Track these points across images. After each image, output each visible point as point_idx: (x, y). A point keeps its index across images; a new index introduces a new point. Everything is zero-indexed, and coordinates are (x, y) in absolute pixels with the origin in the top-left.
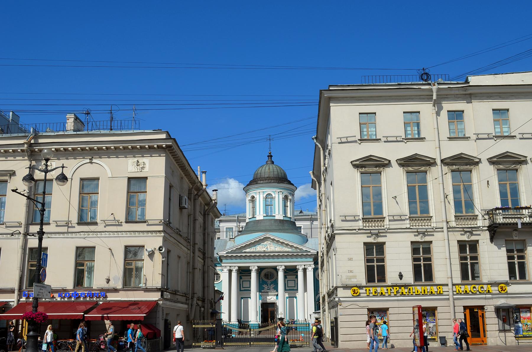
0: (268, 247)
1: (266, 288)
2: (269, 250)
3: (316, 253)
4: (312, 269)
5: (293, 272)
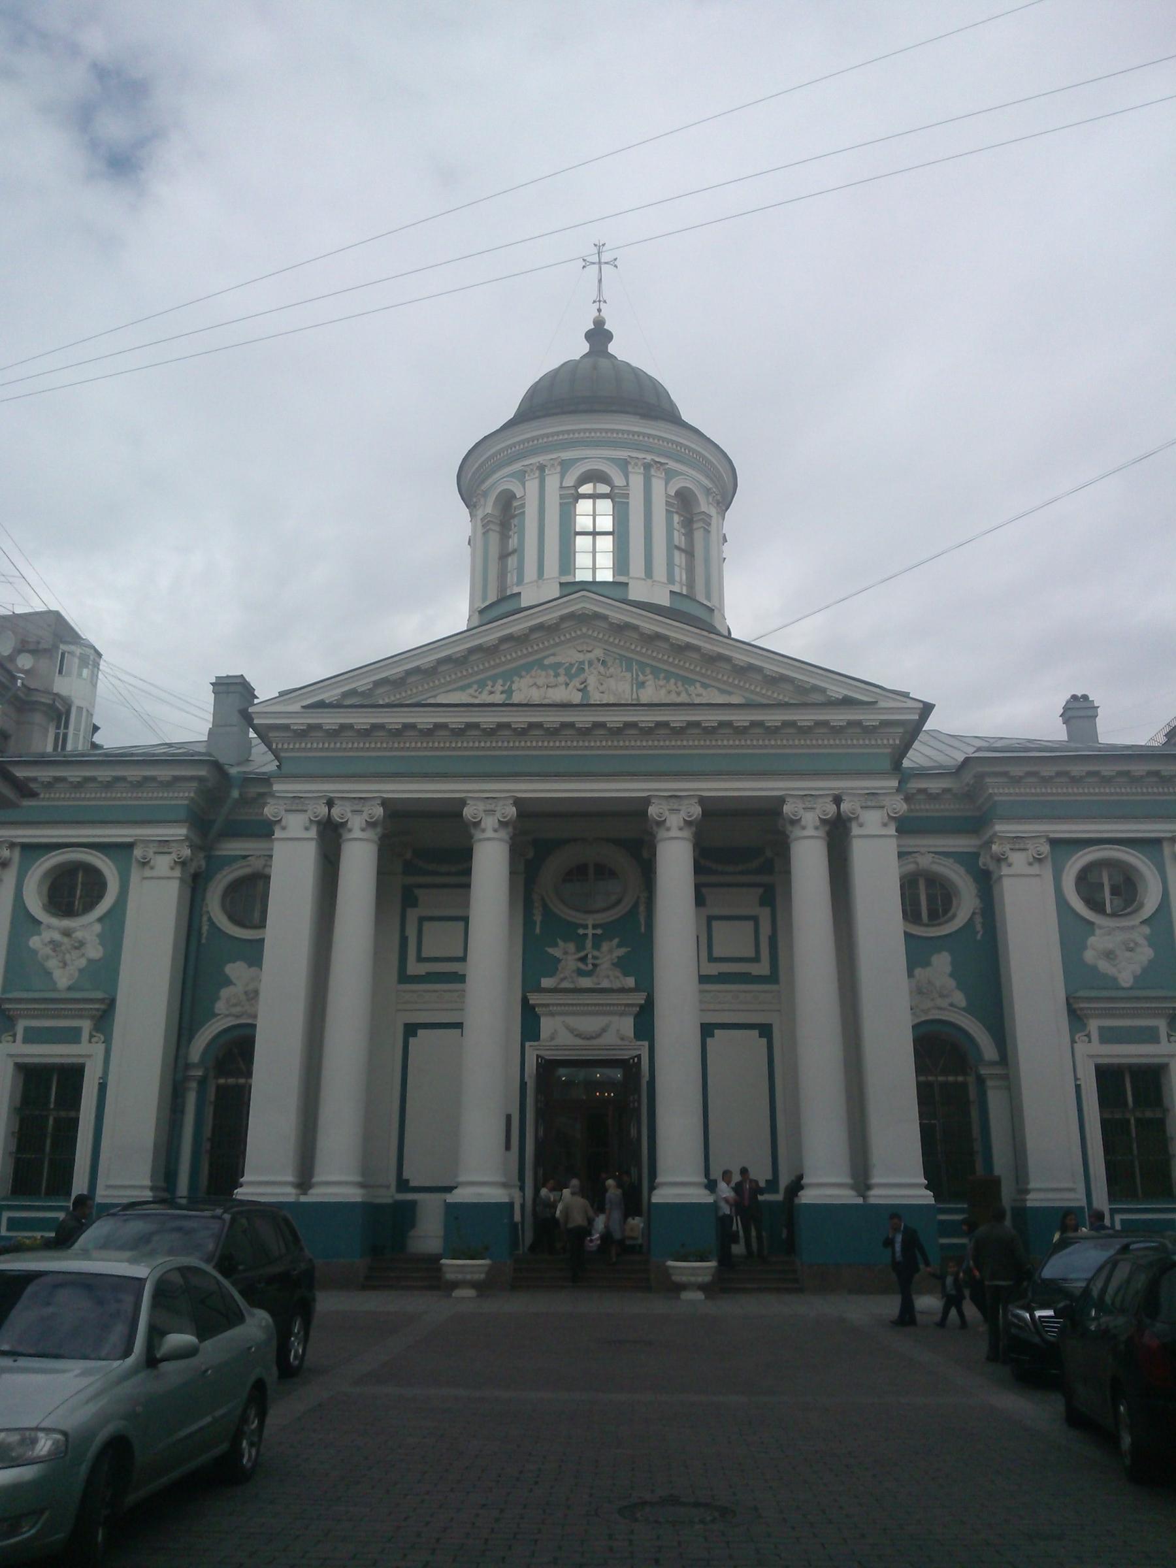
0: (592, 681)
1: (570, 963)
2: (596, 698)
4: (885, 825)
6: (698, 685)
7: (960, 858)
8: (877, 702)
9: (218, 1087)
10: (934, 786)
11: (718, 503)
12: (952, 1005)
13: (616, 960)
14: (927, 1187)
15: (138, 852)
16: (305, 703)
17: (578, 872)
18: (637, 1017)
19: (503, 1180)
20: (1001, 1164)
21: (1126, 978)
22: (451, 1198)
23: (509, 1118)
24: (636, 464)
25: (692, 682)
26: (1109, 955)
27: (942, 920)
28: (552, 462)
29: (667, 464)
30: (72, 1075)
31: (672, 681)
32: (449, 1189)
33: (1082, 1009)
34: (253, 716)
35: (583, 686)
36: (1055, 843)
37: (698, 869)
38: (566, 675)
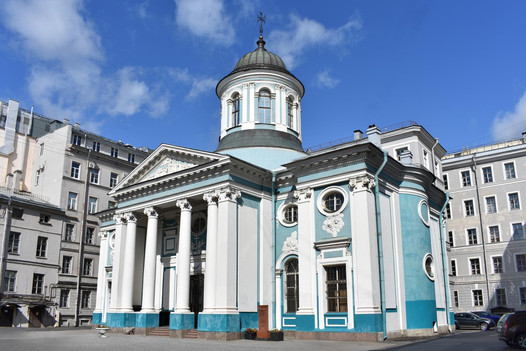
12: (296, 249)
21: (335, 234)
24: (245, 86)
33: (318, 247)
36: (316, 189)
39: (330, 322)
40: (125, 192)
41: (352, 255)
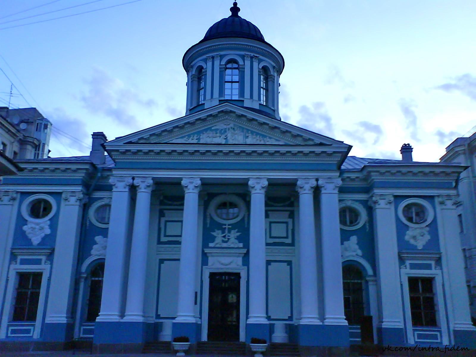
0: (229, 135)
2: (231, 142)
3: (346, 150)
4: (334, 189)
5: (281, 204)
6: (268, 137)
7: (361, 202)
8: (331, 145)
9: (92, 281)
10: (353, 176)
11: (277, 72)
12: (357, 255)
13: (236, 237)
14: (345, 319)
15: (63, 196)
16: (125, 142)
17: (223, 205)
18: (243, 258)
19: (194, 315)
20: (373, 312)
22: (174, 321)
23: (196, 293)
24: (248, 57)
25: (265, 136)
26: (414, 237)
27: (354, 224)
28: (217, 55)
29: (259, 57)
30: (38, 277)
31: (258, 136)
32: (174, 318)
34: (106, 146)
35: (226, 137)
36: (396, 197)
37: (267, 205)
38: (220, 133)
39: (420, 336)
40: (146, 148)
41: (441, 269)
